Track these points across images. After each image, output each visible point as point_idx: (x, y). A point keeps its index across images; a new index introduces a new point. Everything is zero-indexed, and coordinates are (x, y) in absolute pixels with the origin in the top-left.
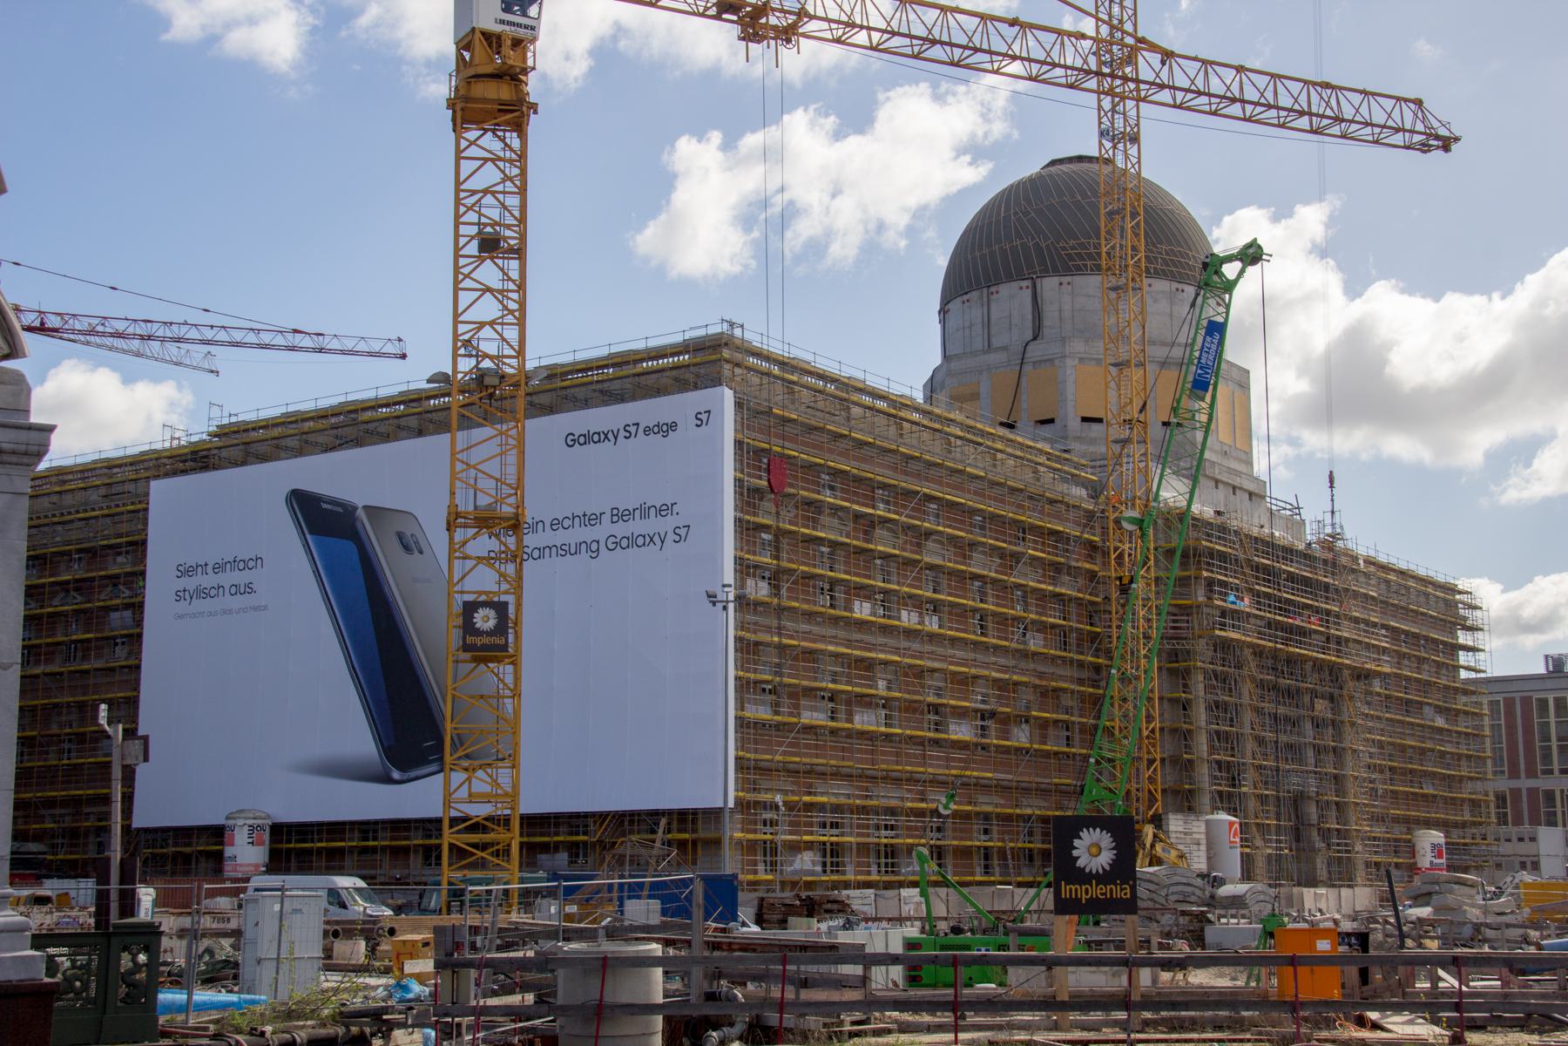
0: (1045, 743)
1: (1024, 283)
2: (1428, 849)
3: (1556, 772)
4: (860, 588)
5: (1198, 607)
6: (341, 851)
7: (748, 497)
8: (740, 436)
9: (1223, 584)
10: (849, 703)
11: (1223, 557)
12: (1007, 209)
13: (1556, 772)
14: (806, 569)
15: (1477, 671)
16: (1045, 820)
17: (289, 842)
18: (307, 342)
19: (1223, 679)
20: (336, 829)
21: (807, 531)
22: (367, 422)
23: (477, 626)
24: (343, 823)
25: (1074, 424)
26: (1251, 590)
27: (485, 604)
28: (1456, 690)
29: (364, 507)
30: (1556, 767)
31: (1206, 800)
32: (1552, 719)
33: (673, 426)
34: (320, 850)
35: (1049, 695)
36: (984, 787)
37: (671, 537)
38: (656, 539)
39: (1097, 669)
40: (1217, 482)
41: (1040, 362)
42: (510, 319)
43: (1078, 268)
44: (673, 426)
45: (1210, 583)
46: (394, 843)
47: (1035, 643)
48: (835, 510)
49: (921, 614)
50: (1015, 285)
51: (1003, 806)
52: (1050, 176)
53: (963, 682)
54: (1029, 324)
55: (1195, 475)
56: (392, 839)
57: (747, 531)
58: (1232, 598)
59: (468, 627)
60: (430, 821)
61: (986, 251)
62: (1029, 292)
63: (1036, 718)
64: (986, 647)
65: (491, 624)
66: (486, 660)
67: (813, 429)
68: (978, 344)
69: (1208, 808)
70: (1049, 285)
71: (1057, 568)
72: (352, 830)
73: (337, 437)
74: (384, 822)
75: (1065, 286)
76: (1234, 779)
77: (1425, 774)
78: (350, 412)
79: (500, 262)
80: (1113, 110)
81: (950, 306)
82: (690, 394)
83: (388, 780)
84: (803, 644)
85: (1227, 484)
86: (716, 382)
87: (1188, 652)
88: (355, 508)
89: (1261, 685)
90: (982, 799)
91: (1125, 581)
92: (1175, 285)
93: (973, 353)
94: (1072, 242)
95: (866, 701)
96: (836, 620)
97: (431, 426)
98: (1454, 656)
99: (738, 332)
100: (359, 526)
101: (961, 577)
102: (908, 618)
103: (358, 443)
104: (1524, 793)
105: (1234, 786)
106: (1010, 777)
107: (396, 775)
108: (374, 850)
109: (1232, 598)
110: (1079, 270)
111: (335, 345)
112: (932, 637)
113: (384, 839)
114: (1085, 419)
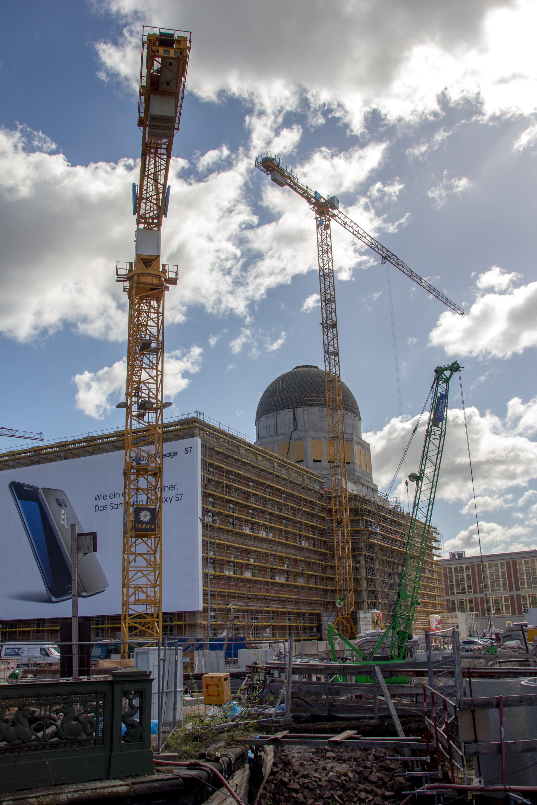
0: (308, 584)
1: (290, 410)
2: (435, 621)
3: (455, 593)
4: (246, 521)
5: (363, 531)
6: (29, 632)
7: (206, 482)
8: (203, 458)
9: (371, 522)
10: (241, 567)
11: (370, 511)
12: (282, 383)
13: (455, 593)
14: (227, 512)
15: (439, 557)
16: (311, 614)
17: (6, 628)
18: (7, 432)
19: (372, 558)
20: (27, 622)
21: (227, 497)
22: (44, 454)
23: (141, 519)
24: (30, 620)
25: (311, 462)
26: (379, 524)
27: (146, 509)
28: (432, 563)
29: (43, 489)
30: (455, 592)
31: (366, 605)
32: (454, 575)
33: (175, 454)
34: (20, 632)
35: (309, 564)
36: (290, 602)
37: (174, 499)
38: (168, 500)
39: (326, 554)
40: (362, 484)
41: (297, 439)
42: (152, 381)
43: (310, 404)
44: (175, 454)
45: (367, 521)
46: (53, 628)
47: (304, 544)
48: (237, 489)
49: (267, 532)
50: (286, 411)
51: (295, 609)
52: (297, 371)
53: (282, 559)
55: (356, 481)
56: (51, 626)
57: (205, 495)
58: (373, 527)
59: (137, 520)
60: (67, 618)
61: (275, 398)
62: (292, 413)
63: (307, 574)
64: (289, 545)
65: (148, 518)
66: (141, 537)
67: (228, 457)
68: (272, 433)
69: (367, 608)
70: (300, 411)
71: (312, 515)
72: (34, 623)
73: (31, 460)
74: (48, 619)
75: (305, 411)
76: (376, 597)
77: (427, 594)
78: (36, 451)
79: (148, 356)
80: (328, 344)
81: (261, 419)
82: (183, 440)
83: (50, 601)
84: (226, 543)
85: (365, 485)
86: (192, 436)
87: (359, 548)
88: (38, 489)
89: (383, 561)
90: (288, 606)
91: (339, 520)
93: (271, 436)
94: (308, 395)
95: (247, 566)
96: (237, 533)
97: (71, 455)
98: (431, 551)
99: (201, 417)
100: (39, 496)
101: (280, 517)
102: (262, 534)
103: (39, 463)
104: (515, 596)
105: (376, 599)
106: (299, 597)
107: (54, 599)
108: (43, 631)
109: (373, 527)
110: (311, 405)
111: (17, 434)
112: (271, 541)
113: (48, 627)
114: (315, 461)
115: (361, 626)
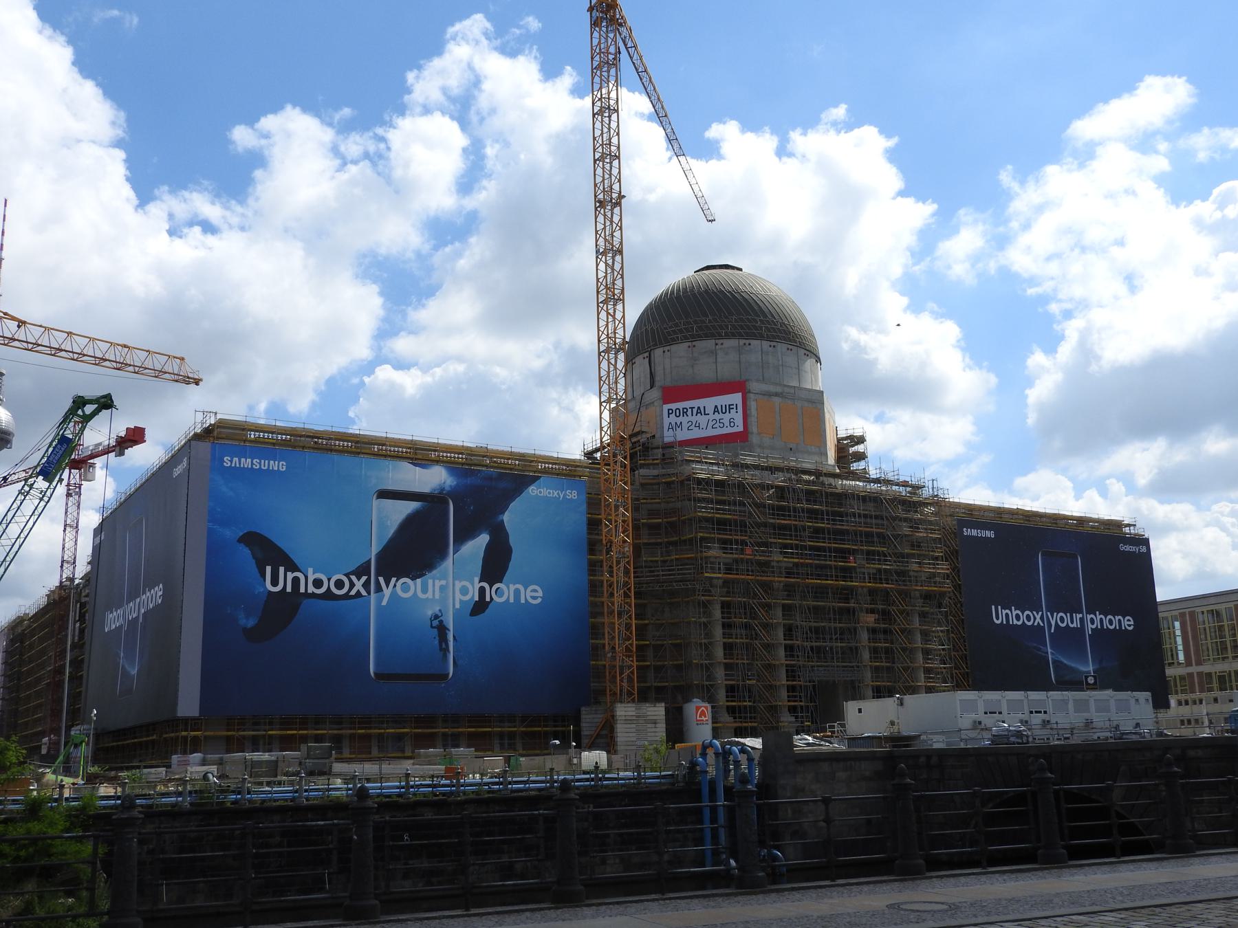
43: (673, 340)
50: (641, 356)
54: (648, 380)
70: (658, 352)
92: (742, 342)
115: (619, 730)
